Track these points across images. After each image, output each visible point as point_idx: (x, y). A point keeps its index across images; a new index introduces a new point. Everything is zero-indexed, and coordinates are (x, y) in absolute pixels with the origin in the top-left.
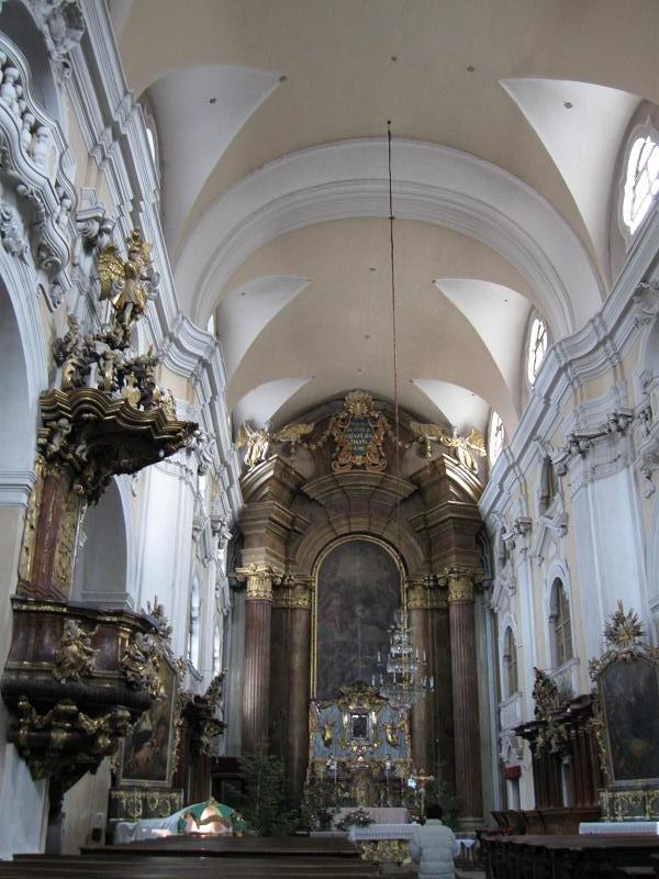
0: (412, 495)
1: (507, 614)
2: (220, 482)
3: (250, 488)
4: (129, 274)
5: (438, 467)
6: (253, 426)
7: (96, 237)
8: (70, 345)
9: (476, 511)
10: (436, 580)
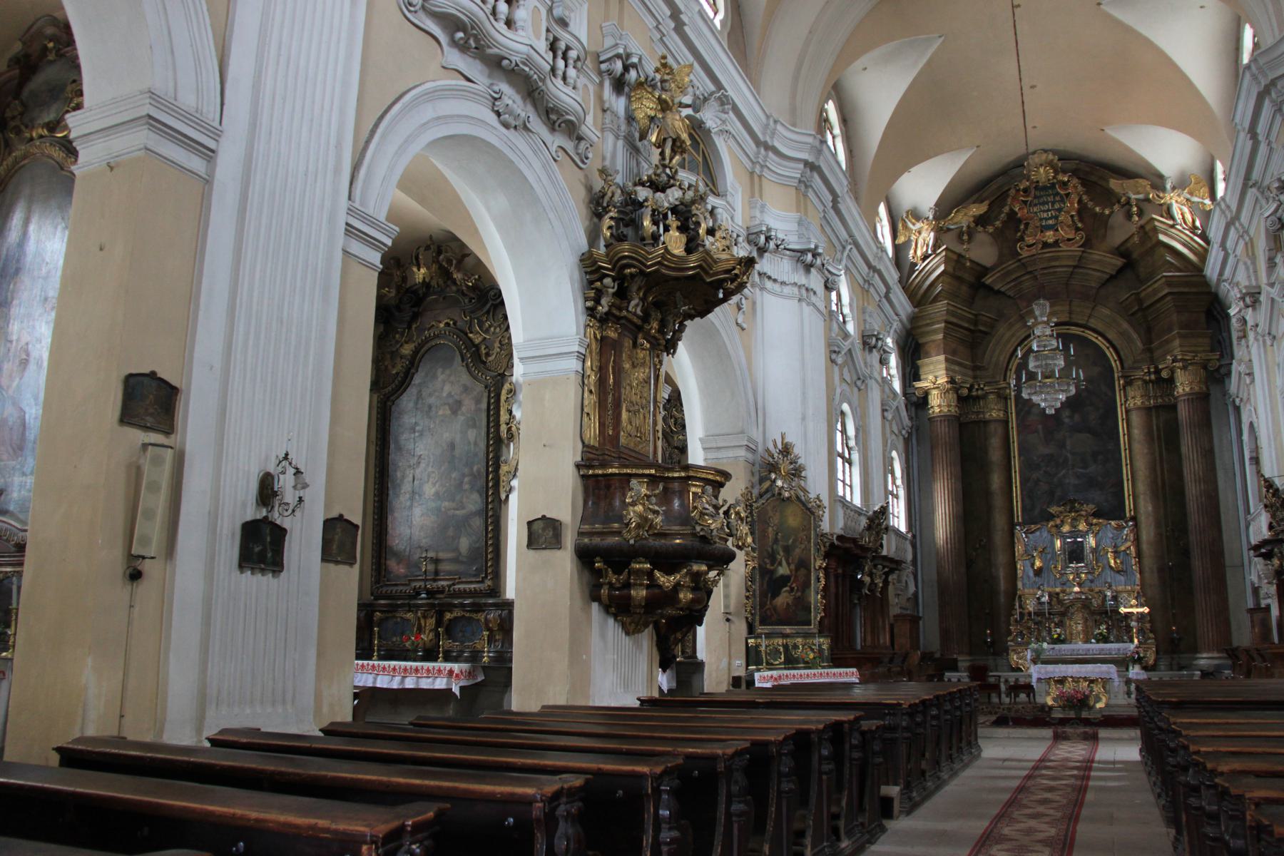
0: (1121, 271)
1: (1248, 407)
2: (872, 290)
3: (920, 287)
4: (664, 105)
5: (1148, 232)
6: (916, 215)
7: (623, 75)
8: (607, 199)
9: (1205, 282)
10: (1158, 372)
